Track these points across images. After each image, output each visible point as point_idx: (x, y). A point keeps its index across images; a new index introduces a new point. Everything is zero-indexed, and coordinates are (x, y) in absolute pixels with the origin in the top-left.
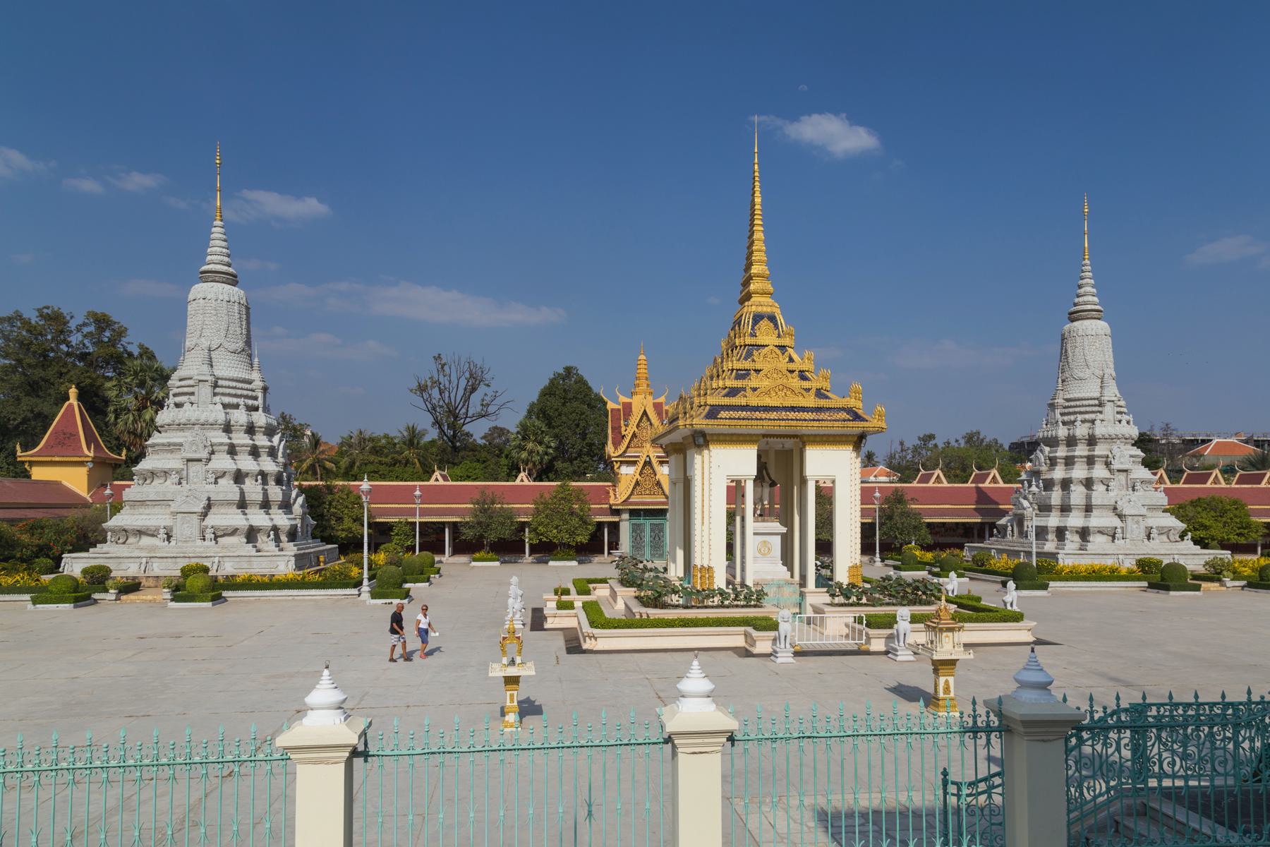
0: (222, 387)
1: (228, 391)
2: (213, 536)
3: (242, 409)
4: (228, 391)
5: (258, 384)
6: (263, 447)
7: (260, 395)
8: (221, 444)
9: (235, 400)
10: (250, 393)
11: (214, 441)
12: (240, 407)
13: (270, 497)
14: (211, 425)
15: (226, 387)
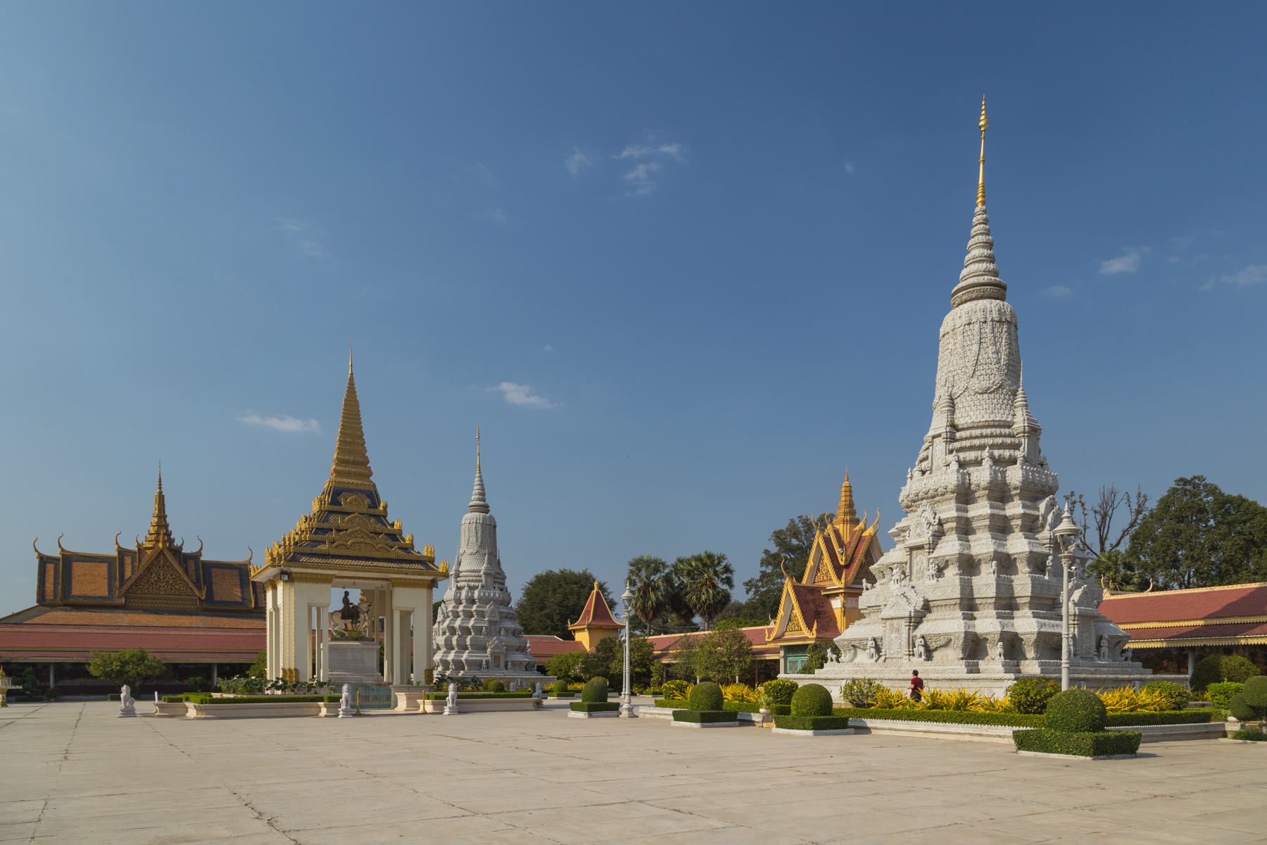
0: (962, 439)
1: (967, 443)
2: (922, 649)
3: (987, 463)
4: (964, 443)
5: (1020, 422)
6: (1013, 518)
7: (1025, 442)
8: (947, 521)
9: (971, 455)
10: (1008, 440)
11: (943, 516)
12: (984, 462)
13: (1015, 592)
14: (942, 495)
15: (966, 438)
